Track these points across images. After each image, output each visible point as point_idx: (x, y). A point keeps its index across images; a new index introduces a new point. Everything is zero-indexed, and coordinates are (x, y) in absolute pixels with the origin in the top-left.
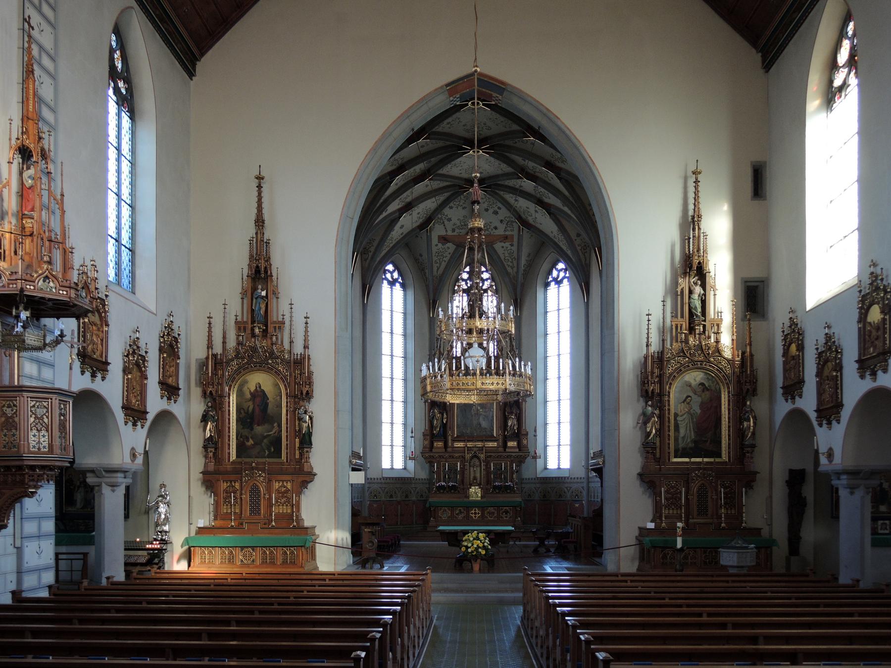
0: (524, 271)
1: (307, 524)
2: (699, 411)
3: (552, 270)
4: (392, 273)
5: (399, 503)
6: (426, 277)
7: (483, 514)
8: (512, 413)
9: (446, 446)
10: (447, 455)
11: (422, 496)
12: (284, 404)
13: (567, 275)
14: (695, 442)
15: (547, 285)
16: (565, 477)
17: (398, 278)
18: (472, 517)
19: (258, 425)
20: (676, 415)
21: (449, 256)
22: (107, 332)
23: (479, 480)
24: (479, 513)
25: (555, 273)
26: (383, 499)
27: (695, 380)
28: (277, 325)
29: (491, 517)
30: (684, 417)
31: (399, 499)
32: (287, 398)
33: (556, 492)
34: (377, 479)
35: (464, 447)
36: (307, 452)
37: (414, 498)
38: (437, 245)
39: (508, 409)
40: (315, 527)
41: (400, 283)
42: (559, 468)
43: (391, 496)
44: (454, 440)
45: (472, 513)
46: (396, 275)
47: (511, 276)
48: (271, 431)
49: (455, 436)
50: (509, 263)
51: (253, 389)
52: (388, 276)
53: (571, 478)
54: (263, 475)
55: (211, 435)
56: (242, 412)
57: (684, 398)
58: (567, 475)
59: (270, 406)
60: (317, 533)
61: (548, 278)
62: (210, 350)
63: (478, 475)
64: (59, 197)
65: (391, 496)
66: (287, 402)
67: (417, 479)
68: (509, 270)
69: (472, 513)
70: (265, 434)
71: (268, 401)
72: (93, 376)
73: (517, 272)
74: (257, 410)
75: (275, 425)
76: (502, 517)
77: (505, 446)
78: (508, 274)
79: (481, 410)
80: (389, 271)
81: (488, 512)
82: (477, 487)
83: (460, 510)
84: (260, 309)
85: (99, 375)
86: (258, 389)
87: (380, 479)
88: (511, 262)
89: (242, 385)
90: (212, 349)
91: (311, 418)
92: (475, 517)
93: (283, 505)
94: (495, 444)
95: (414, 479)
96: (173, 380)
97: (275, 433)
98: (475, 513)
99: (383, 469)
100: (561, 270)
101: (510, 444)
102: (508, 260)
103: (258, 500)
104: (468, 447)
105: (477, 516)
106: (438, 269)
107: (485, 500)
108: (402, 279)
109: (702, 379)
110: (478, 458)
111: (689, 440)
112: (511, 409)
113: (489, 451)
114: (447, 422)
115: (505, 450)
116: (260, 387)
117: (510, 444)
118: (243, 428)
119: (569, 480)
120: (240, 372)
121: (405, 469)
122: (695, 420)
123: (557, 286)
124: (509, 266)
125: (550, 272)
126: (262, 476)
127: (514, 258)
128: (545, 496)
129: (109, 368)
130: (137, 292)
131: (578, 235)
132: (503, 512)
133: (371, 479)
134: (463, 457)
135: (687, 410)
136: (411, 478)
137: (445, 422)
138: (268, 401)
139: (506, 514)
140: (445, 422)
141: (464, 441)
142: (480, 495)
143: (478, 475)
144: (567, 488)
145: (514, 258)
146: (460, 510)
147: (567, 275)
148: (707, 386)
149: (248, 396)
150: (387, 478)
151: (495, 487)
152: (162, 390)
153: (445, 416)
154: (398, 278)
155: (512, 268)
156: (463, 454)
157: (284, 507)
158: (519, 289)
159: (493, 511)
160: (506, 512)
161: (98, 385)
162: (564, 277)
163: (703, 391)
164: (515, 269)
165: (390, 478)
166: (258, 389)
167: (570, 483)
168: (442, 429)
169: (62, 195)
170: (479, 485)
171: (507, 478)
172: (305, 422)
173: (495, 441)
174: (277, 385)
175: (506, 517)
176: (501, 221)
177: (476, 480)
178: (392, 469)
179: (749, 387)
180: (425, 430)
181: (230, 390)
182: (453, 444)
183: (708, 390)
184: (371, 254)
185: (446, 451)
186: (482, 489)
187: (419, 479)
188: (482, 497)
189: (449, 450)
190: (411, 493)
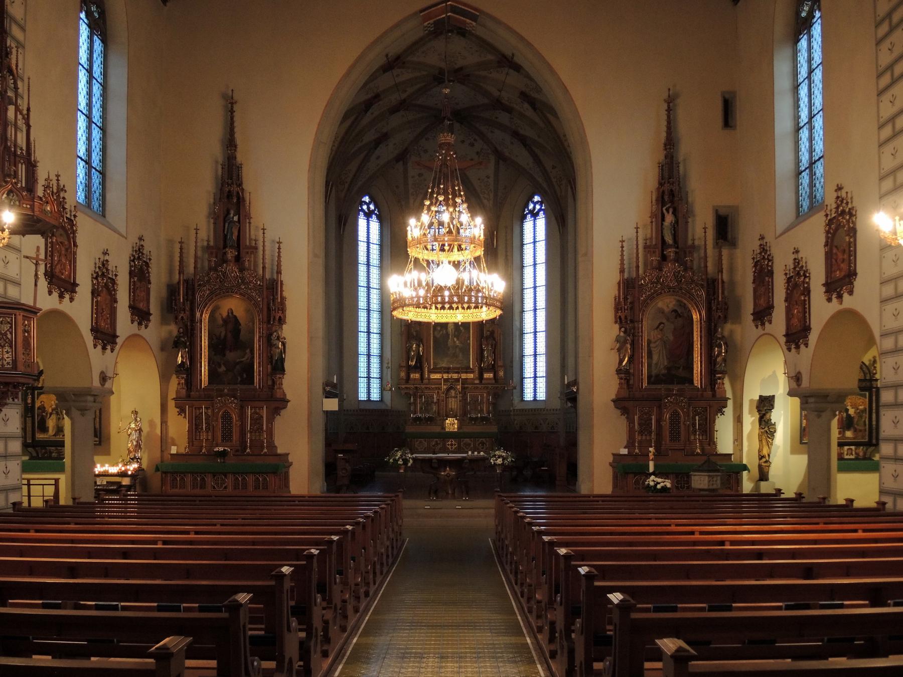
1: (279, 451)
2: (671, 338)
4: (368, 204)
7: (459, 444)
10: (423, 386)
12: (257, 330)
14: (668, 369)
15: (524, 217)
16: (541, 409)
17: (375, 210)
19: (231, 351)
20: (649, 342)
22: (75, 253)
24: (455, 445)
25: (531, 206)
27: (668, 306)
28: (250, 250)
30: (657, 343)
32: (260, 324)
35: (441, 379)
36: (280, 378)
38: (413, 177)
40: (289, 454)
41: (376, 214)
44: (430, 372)
46: (372, 207)
48: (243, 357)
49: (432, 367)
51: (225, 314)
52: (365, 207)
53: (547, 410)
54: (235, 401)
55: (182, 361)
56: (214, 338)
57: (657, 324)
58: (543, 407)
59: (242, 333)
60: (290, 461)
61: (525, 211)
62: (182, 275)
64: (25, 112)
66: (260, 329)
70: (238, 360)
71: (240, 327)
72: (61, 296)
74: (229, 335)
75: (248, 351)
77: (481, 377)
79: (457, 342)
80: (365, 203)
81: (465, 444)
83: (436, 441)
84: (232, 234)
85: (67, 296)
86: (230, 314)
89: (214, 311)
90: (183, 274)
91: (284, 344)
93: (256, 432)
94: (471, 376)
96: (143, 305)
97: (247, 359)
100: (537, 202)
101: (486, 376)
103: (230, 426)
105: (454, 447)
107: (461, 431)
108: (378, 211)
109: (674, 305)
111: (662, 367)
113: (465, 381)
116: (232, 313)
117: (486, 376)
118: (215, 355)
120: (212, 298)
121: (382, 400)
122: (668, 347)
123: (533, 219)
125: (527, 206)
126: (234, 403)
129: (77, 289)
130: (107, 216)
131: (554, 167)
132: (480, 443)
133: (347, 410)
134: (439, 389)
135: (659, 336)
138: (240, 327)
142: (456, 426)
147: (543, 208)
148: (679, 312)
149: (220, 322)
150: (363, 410)
151: (471, 419)
152: (132, 314)
154: (375, 210)
157: (257, 434)
159: (469, 442)
161: (65, 306)
162: (540, 210)
163: (676, 318)
166: (230, 314)
169: (28, 110)
170: (455, 416)
172: (279, 348)
173: (472, 372)
174: (247, 311)
176: (477, 153)
178: (369, 400)
179: (720, 314)
181: (201, 315)
182: (429, 376)
183: (680, 316)
184: (347, 186)
188: (458, 428)
189: (425, 381)
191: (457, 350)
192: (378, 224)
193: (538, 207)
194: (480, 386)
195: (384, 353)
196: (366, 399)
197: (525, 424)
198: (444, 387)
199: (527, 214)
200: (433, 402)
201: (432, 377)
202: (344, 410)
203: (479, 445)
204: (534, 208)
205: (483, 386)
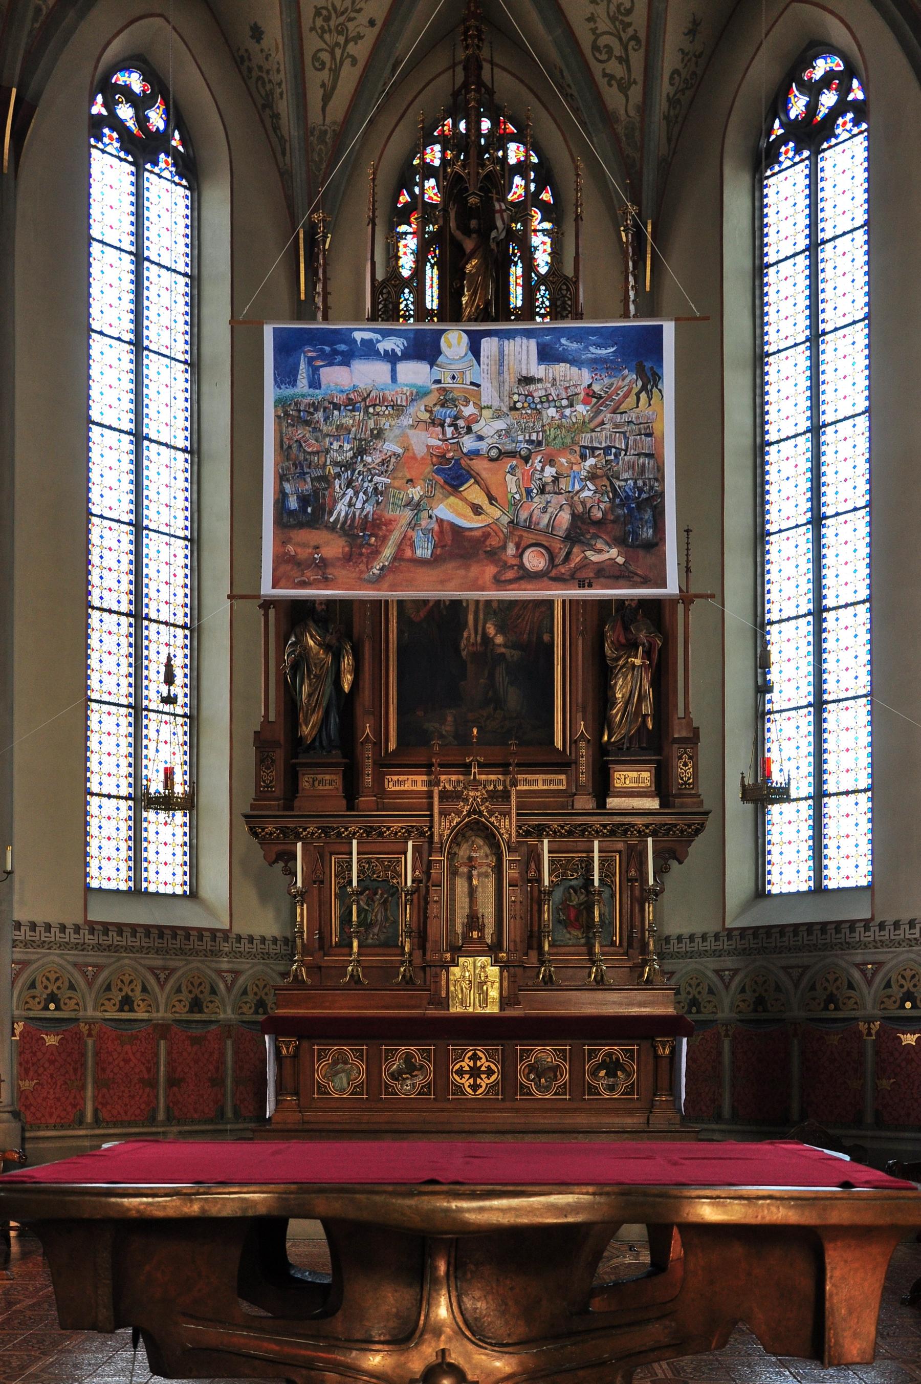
0: (673, 102)
3: (789, 90)
4: (140, 104)
5: (163, 1030)
6: (281, 139)
7: (508, 1075)
8: (631, 646)
9: (351, 791)
11: (261, 1004)
13: (857, 94)
18: (460, 1089)
21: (371, 35)
23: (489, 931)
24: (490, 1072)
25: (798, 106)
26: (90, 1012)
29: (547, 1089)
31: (161, 1015)
33: (813, 988)
34: (63, 928)
37: (227, 1014)
39: (611, 635)
42: (819, 890)
43: (127, 1003)
45: (460, 1072)
46: (156, 119)
47: (620, 129)
50: (616, 69)
63: (487, 910)
65: (127, 1003)
67: (239, 938)
68: (613, 97)
69: (460, 1072)
73: (645, 108)
76: (592, 1090)
78: (607, 118)
79: (499, 640)
81: (532, 1068)
82: (482, 960)
83: (408, 1058)
87: (77, 929)
88: (620, 59)
92: (475, 1087)
94: (560, 781)
95: (226, 939)
98: (475, 1072)
99: (87, 888)
102: (609, 49)
104: (444, 795)
106: (326, 99)
107: (510, 1013)
110: (490, 837)
112: (626, 629)
114: (355, 684)
115: (602, 804)
119: (873, 933)
121: (193, 895)
124: (611, 77)
127: (635, 37)
128: (760, 1002)
132: (599, 1067)
133: (33, 926)
136: (213, 932)
137: (346, 688)
139: (611, 1074)
140: (346, 688)
141: (427, 768)
142: (494, 993)
143: (487, 910)
144: (860, 966)
145: (635, 37)
146: (408, 1058)
150: (106, 927)
153: (347, 662)
155: (624, 88)
156: (424, 824)
158: (649, 177)
160: (612, 1067)
164: (636, 93)
165: (120, 928)
167: (879, 944)
168: (334, 719)
170: (493, 950)
171: (612, 923)
175: (611, 1088)
177: (481, 929)
180: (266, 721)
182: (379, 781)
185: (351, 807)
186: (504, 966)
187: (251, 939)
188: (504, 1002)
190: (213, 991)
191: (500, 675)
192: (181, 191)
193: (829, 99)
194: (596, 821)
195: (205, 704)
196: (123, 887)
197: (778, 989)
198: (442, 828)
199: (782, 140)
200: (394, 891)
201: (391, 787)
202: (18, 925)
203: (594, 1073)
204: (812, 108)
205: (606, 820)
